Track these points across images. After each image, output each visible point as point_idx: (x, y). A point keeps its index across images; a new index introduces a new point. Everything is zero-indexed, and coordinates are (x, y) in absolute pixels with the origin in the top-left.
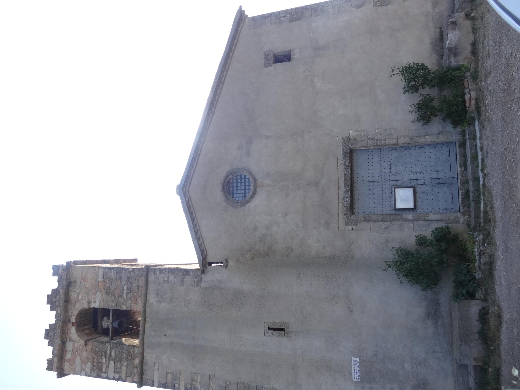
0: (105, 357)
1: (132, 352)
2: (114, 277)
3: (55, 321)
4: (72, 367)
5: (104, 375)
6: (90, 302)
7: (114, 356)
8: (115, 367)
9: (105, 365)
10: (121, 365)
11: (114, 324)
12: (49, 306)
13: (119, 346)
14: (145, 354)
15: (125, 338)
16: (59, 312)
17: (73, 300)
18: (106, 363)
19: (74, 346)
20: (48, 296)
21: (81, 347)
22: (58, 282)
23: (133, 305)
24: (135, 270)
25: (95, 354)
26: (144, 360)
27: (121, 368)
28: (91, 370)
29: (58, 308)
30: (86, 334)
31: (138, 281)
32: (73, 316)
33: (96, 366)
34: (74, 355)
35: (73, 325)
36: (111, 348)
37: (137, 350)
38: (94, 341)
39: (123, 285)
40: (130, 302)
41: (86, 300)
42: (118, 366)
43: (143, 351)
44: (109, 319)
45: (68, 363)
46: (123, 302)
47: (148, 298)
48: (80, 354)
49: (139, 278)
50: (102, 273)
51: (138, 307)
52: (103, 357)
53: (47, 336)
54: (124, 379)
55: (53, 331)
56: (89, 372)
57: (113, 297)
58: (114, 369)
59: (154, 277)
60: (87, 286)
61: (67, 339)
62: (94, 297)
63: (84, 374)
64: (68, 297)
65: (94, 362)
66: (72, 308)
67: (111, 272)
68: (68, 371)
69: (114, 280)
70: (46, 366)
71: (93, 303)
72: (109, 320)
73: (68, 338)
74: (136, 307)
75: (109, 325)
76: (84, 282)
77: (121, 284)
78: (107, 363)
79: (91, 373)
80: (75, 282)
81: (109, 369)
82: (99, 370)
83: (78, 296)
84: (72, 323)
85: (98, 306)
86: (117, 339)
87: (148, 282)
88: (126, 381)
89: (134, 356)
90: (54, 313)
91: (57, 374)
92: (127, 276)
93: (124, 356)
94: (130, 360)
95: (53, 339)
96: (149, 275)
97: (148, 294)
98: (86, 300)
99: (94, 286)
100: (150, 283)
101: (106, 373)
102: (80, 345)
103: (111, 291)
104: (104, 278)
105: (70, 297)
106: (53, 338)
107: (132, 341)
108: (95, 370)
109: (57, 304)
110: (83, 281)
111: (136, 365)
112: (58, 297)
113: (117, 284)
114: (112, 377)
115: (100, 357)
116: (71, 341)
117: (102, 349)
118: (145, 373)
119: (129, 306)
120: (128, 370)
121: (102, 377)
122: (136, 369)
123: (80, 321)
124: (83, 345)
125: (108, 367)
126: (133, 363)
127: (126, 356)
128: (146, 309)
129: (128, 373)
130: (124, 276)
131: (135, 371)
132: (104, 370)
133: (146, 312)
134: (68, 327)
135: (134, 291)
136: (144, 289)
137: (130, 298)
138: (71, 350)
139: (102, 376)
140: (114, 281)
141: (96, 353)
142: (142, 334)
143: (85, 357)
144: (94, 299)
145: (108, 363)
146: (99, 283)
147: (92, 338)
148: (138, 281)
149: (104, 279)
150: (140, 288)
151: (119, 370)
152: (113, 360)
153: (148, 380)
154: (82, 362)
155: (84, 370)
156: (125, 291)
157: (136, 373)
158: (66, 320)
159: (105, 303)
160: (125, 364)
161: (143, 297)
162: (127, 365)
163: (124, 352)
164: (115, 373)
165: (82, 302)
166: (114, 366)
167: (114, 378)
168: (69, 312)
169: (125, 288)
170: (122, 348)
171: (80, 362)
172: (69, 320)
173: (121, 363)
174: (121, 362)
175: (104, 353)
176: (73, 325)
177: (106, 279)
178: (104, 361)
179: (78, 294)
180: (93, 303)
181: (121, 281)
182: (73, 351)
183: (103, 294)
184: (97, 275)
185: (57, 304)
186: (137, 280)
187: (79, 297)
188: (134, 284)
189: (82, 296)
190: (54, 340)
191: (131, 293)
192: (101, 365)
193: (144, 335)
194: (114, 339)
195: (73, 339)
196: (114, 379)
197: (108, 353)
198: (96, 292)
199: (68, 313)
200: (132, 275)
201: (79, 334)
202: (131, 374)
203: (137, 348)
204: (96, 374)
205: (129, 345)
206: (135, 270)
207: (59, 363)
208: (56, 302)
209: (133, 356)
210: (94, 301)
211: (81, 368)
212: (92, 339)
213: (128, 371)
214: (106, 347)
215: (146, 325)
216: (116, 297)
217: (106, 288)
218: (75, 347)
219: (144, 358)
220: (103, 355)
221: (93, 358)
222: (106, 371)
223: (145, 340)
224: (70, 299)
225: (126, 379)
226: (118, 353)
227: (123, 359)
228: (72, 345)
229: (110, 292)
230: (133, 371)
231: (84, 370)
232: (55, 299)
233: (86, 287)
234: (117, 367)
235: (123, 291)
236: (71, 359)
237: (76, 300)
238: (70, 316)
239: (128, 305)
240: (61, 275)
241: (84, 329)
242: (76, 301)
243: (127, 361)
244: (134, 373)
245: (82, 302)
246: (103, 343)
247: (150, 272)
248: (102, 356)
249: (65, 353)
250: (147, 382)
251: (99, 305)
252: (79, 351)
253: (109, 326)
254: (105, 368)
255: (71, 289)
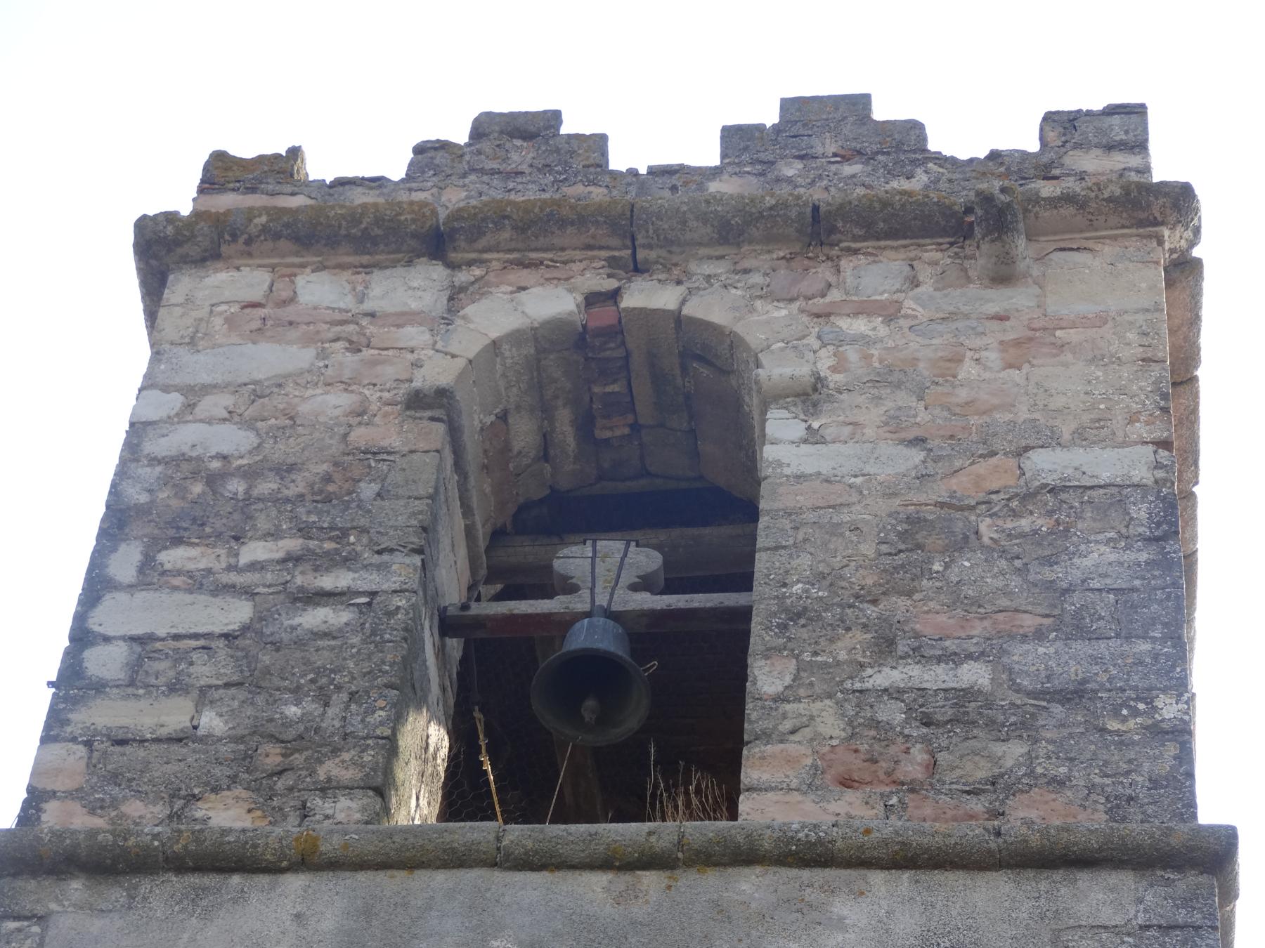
0: (292, 559)
1: (322, 777)
2: (1076, 576)
3: (633, 173)
4: (218, 322)
5: (125, 564)
6: (815, 405)
7: (293, 628)
8: (193, 643)
9: (217, 566)
10: (204, 691)
11: (600, 621)
12: (770, 117)
13: (389, 657)
14: (295, 883)
15: (444, 752)
16: (714, 187)
17: (832, 279)
18: (230, 568)
19: (405, 318)
20: (861, 103)
21: (390, 372)
22: (994, 156)
23: (802, 749)
24: (1172, 749)
25: (328, 479)
26: (236, 879)
27: (176, 688)
28: (176, 461)
29: (753, 180)
30: (503, 417)
31: (1059, 783)
32: (681, 290)
33: (214, 492)
34: (326, 327)
35: (592, 299)
36: (373, 594)
37: (341, 817)
38: (439, 468)
39: (1003, 652)
40: (830, 723)
41: (834, 369)
42: (196, 670)
43: (334, 865)
44: (645, 584)
45: (257, 295)
46: (825, 665)
47: (877, 878)
48: (329, 372)
49: (1091, 788)
50: (1105, 476)
51: (770, 795)
52: (292, 544)
53: (502, 132)
54: (67, 722)
55: (539, 163)
56: (158, 446)
57: (869, 581)
58: (177, 637)
59: (1118, 920)
60: (969, 370)
61: (470, 264)
62: (869, 432)
63: (151, 414)
64: (855, 239)
65: (250, 474)
66: (756, 278)
67: (1128, 547)
68: (189, 300)
69: (1048, 574)
70: (245, 149)
71: (809, 428)
72: (634, 588)
73: (478, 272)
74: (779, 776)
75: (585, 593)
76: (1002, 343)
77: (1012, 637)
78: (233, 578)
79: (154, 461)
80: (1003, 276)
81: (179, 597)
82: (173, 524)
83: (864, 309)
84: (614, 295)
85: (780, 464)
86: (441, 676)
87: (1058, 875)
88: (47, 739)
89: (291, 789)
90: (708, 154)
91: (171, 217)
92: (1103, 678)
93: (293, 711)
94: (247, 758)
95: (473, 170)
96: (1125, 880)
97: (923, 876)
98: (834, 369)
99: (974, 420)
100: (1043, 886)
101: (141, 570)
102: (417, 365)
103: (930, 561)
104: (1063, 496)
105: (856, 252)
106: (482, 171)
107: (423, 802)
108: (181, 491)
109: (791, 169)
110: (1011, 336)
111: (199, 814)
112: (848, 170)
113: (1004, 602)
114: (102, 620)
115: (294, 518)
116: (451, 299)
117: (364, 530)
118: (116, 894)
119: (784, 716)
120: (154, 747)
121: (114, 549)
122: (160, 810)
123: (627, 358)
124: (417, 384)
125: (200, 583)
126: (216, 790)
127: (288, 723)
128: (758, 869)
129: (128, 749)
130: (1096, 660)
131: (133, 808)
132: (172, 557)
133: (730, 870)
134: (576, 267)
135: (940, 757)
136: (974, 832)
137: (874, 724)
138: (368, 306)
139: (123, 547)
140: (1031, 577)
141: (331, 488)
142: (498, 839)
143: (304, 408)
144: (847, 430)
145: (230, 589)
146: (1012, 462)
147: (472, 468)
148: (1059, 783)
149: (1053, 490)
150: (977, 805)
151: (162, 680)
152: (261, 619)
153: (36, 929)
154: (258, 392)
155: (190, 407)
156: (936, 677)
157: (122, 816)
158: (640, 240)
159: (810, 517)
160: (211, 721)
161: (888, 828)
162: (201, 740)
163: (326, 705)
164: (138, 649)
165: (812, 341)
166: (201, 630)
167: (93, 644)
168: (722, 257)
169: (975, 674)
170: (363, 683)
171: (261, 376)
172: (638, 269)
173: (227, 685)
174: (233, 691)
175: (328, 546)
176: (592, 299)
177: (1050, 513)
178: (255, 551)
179: (890, 313)
180: (809, 428)
181: (1039, 635)
182: (364, 322)
183: (895, 495)
184: (1081, 437)
185: (791, 169)
186: (1063, 770)
187: (857, 314)
188: (1014, 751)
189: (863, 336)
190: (464, 176)
191: (925, 730)
192: (219, 536)
193: (493, 864)
194: (443, 646)
195: (470, 310)
196: (82, 637)
197: (327, 582)
198: (919, 441)
199: (703, 251)
200: (1113, 725)
201: (506, 348)
202: (114, 777)
203: (364, 809)
204: (144, 498)
205: (391, 748)
206: (1172, 749)
207: (264, 219)
208: (801, 158)
209: (280, 784)
210: (829, 433)
211: (206, 389)
212: (459, 466)
213: (142, 753)
214: (386, 557)
215: (599, 880)
216: (874, 602)
217: (958, 515)
218: (398, 326)
219: (264, 880)
220: (313, 544)
221: (285, 470)
222: (164, 573)
223: (440, 879)
224: (835, 251)
225: (74, 740)
226: (326, 653)
227: (260, 700)
228: (414, 305)
229: (917, 556)
230: (140, 795)
231: (190, 407)
232: (831, 148)
233: (959, 360)
234: (195, 656)
235: (939, 660)
236: (290, 309)
237: (828, 299)
238: (676, 272)
239: (801, 707)
240: (1056, 172)
241: (545, 410)
242: (821, 301)
243: (239, 739)
244: (115, 803)
245: (816, 344)
246: (425, 529)
247: (1169, 883)
248: (304, 531)
249: (342, 267)
250: (17, 918)
251: (787, 471)
252: (357, 357)
253: (571, 589)
254: (191, 566)
255: (933, 256)
